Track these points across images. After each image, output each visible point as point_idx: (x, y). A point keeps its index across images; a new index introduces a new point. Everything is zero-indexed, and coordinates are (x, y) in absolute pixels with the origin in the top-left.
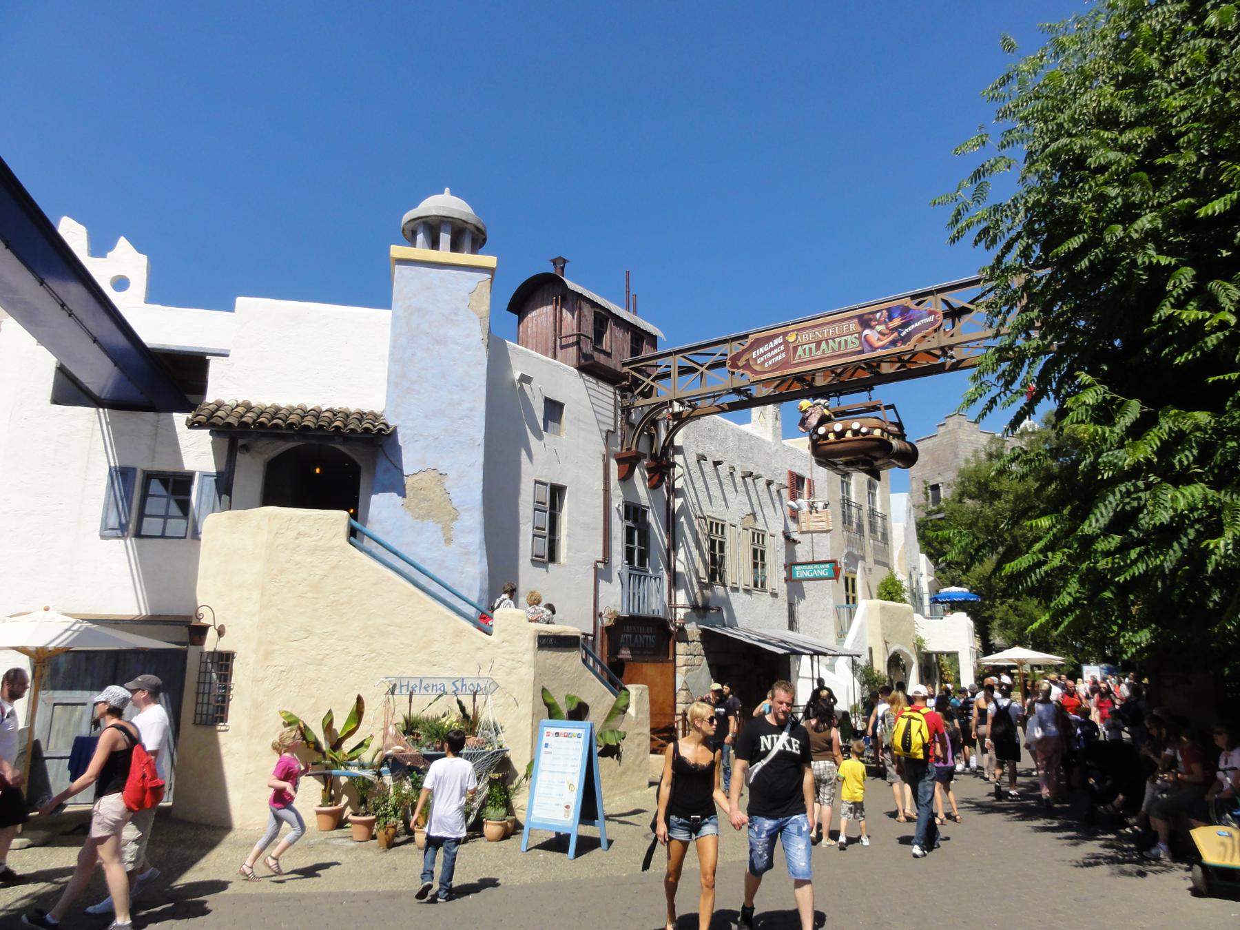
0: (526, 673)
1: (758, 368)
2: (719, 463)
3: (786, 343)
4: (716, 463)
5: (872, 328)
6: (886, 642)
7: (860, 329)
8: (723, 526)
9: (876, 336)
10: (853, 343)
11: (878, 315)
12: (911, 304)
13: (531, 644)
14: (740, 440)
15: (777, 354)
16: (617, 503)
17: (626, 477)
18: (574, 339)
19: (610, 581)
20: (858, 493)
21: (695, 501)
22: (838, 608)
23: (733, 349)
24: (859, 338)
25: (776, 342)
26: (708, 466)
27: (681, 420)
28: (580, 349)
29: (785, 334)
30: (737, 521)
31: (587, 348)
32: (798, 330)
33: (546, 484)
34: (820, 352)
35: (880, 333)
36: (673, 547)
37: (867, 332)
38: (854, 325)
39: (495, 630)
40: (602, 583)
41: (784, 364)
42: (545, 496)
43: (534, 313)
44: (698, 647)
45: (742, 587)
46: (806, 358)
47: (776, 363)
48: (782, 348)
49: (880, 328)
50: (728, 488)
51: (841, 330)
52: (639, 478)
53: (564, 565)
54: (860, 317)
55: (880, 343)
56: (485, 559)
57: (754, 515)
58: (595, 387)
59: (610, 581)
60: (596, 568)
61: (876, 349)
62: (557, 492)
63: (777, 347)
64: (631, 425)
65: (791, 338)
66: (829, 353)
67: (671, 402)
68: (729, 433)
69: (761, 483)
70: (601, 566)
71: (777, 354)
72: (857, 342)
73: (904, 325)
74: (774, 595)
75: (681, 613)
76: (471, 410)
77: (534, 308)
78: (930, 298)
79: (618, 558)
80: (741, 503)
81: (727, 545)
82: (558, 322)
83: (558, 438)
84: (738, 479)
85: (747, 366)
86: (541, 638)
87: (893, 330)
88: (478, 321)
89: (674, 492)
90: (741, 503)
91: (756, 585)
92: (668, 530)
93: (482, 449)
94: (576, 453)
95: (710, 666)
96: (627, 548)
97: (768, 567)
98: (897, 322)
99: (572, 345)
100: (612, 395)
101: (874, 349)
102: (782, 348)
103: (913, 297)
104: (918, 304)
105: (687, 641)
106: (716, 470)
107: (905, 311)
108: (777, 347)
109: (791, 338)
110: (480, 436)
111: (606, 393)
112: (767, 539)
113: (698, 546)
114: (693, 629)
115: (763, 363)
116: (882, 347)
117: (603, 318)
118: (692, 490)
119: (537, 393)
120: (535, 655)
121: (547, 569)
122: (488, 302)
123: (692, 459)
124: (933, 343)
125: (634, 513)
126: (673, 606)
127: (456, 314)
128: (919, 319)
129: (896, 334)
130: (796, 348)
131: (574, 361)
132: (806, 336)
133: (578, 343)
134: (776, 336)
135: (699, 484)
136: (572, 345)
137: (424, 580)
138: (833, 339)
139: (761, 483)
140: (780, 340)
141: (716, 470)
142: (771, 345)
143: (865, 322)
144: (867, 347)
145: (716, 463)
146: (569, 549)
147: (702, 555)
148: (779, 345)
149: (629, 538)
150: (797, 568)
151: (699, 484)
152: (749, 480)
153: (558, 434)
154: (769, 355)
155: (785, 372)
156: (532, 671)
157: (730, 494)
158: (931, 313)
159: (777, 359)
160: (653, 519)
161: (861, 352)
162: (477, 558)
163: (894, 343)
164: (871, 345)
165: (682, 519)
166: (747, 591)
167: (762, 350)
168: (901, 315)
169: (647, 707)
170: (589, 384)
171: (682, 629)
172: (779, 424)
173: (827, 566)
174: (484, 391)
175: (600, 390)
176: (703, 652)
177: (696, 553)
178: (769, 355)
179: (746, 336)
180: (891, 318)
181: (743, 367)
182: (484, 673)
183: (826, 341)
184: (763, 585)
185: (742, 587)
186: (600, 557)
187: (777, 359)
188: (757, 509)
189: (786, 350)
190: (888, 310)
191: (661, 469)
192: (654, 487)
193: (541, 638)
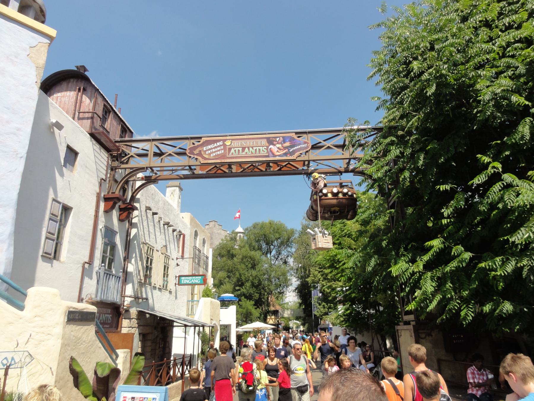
0: (54, 345)
1: (207, 156)
2: (156, 214)
3: (224, 145)
4: (154, 214)
5: (275, 145)
6: (211, 319)
7: (267, 145)
8: (153, 250)
9: (276, 149)
10: (263, 151)
11: (278, 139)
12: (295, 136)
13: (62, 318)
14: (164, 204)
15: (219, 150)
16: (101, 225)
17: (107, 211)
18: (90, 115)
19: (91, 278)
20: (200, 244)
21: (142, 233)
22: (188, 301)
23: (187, 145)
24: (267, 149)
25: (218, 144)
26: (150, 213)
27: (149, 180)
28: (93, 123)
29: (225, 140)
30: (159, 249)
31: (98, 123)
32: (232, 140)
33: (59, 203)
34: (244, 153)
35: (278, 148)
36: (127, 258)
37: (271, 146)
38: (264, 142)
39: (28, 303)
40: (86, 279)
41: (223, 156)
42: (58, 210)
43: (59, 94)
44: (135, 322)
45: (158, 286)
46: (236, 155)
47: (218, 155)
48: (222, 147)
49: (278, 146)
50: (157, 229)
51: (257, 143)
52: (115, 214)
53: (62, 263)
54: (268, 139)
55: (278, 154)
56: (12, 248)
57: (166, 246)
58: (99, 151)
59: (91, 278)
60: (83, 267)
61: (276, 156)
62: (66, 209)
63: (219, 146)
64: (116, 181)
65: (228, 143)
66: (249, 154)
67: (147, 168)
68: (160, 199)
69: (171, 229)
70: (87, 266)
71: (219, 150)
72: (266, 151)
73: (292, 146)
74: (170, 292)
75: (128, 301)
76: (19, 129)
77: (59, 92)
78: (305, 135)
79: (97, 262)
80: (162, 239)
81: (153, 261)
82: (78, 103)
83: (72, 174)
84: (162, 226)
85: (200, 154)
86: (70, 313)
87: (285, 148)
88: (34, 68)
89: (132, 225)
90: (162, 239)
91: (163, 287)
92: (125, 250)
93: (22, 162)
94: (82, 185)
95: (140, 334)
96: (103, 256)
97: (169, 276)
98: (287, 144)
99: (88, 118)
100: (106, 159)
101: (274, 156)
102: (222, 147)
103: (296, 133)
104: (299, 137)
105: (130, 319)
106: (153, 217)
107: (292, 139)
108: (219, 146)
109: (228, 143)
110: (23, 149)
111: (104, 156)
112: (171, 260)
113: (141, 259)
114: (134, 312)
115: (210, 154)
116: (279, 156)
117: (108, 110)
118: (141, 227)
119: (63, 140)
120: (64, 327)
121: (52, 264)
122: (45, 58)
123: (143, 209)
124: (304, 158)
125: (109, 233)
126: (123, 296)
127: (16, 57)
128: (300, 144)
129: (287, 150)
130: (230, 149)
131: (88, 129)
132: (236, 144)
133: (92, 118)
134: (219, 141)
135: (145, 224)
136: (88, 118)
137: (165, 168)
138: (252, 147)
139: (171, 229)
140: (221, 143)
141: (153, 217)
142: (215, 145)
143: (271, 142)
144: (271, 154)
145: (154, 214)
146: (68, 252)
147: (142, 264)
148: (220, 146)
149: (105, 252)
150: (183, 278)
151: (145, 224)
152: (166, 226)
153: (72, 171)
154: (214, 150)
155: (223, 161)
156: (59, 343)
157: (158, 234)
158: (305, 143)
159: (218, 153)
160: (118, 240)
161: (268, 156)
162: (5, 246)
163: (285, 154)
164: (273, 154)
165: (135, 242)
166: (160, 289)
167: (209, 147)
168: (290, 141)
169: (128, 365)
170: (95, 147)
171: (127, 311)
172: (180, 200)
173: (200, 277)
174: (32, 119)
175: (102, 154)
176: (137, 325)
177: (140, 263)
178: (214, 150)
179: (200, 138)
180: (284, 142)
181: (197, 155)
182: (21, 347)
183: (248, 148)
184: (166, 287)
185: (158, 286)
186: (87, 260)
187: (218, 153)
188: (168, 243)
189: (224, 149)
190: (283, 137)
191: (127, 210)
192: (121, 220)
193: (70, 313)
